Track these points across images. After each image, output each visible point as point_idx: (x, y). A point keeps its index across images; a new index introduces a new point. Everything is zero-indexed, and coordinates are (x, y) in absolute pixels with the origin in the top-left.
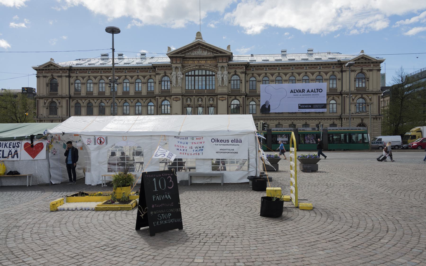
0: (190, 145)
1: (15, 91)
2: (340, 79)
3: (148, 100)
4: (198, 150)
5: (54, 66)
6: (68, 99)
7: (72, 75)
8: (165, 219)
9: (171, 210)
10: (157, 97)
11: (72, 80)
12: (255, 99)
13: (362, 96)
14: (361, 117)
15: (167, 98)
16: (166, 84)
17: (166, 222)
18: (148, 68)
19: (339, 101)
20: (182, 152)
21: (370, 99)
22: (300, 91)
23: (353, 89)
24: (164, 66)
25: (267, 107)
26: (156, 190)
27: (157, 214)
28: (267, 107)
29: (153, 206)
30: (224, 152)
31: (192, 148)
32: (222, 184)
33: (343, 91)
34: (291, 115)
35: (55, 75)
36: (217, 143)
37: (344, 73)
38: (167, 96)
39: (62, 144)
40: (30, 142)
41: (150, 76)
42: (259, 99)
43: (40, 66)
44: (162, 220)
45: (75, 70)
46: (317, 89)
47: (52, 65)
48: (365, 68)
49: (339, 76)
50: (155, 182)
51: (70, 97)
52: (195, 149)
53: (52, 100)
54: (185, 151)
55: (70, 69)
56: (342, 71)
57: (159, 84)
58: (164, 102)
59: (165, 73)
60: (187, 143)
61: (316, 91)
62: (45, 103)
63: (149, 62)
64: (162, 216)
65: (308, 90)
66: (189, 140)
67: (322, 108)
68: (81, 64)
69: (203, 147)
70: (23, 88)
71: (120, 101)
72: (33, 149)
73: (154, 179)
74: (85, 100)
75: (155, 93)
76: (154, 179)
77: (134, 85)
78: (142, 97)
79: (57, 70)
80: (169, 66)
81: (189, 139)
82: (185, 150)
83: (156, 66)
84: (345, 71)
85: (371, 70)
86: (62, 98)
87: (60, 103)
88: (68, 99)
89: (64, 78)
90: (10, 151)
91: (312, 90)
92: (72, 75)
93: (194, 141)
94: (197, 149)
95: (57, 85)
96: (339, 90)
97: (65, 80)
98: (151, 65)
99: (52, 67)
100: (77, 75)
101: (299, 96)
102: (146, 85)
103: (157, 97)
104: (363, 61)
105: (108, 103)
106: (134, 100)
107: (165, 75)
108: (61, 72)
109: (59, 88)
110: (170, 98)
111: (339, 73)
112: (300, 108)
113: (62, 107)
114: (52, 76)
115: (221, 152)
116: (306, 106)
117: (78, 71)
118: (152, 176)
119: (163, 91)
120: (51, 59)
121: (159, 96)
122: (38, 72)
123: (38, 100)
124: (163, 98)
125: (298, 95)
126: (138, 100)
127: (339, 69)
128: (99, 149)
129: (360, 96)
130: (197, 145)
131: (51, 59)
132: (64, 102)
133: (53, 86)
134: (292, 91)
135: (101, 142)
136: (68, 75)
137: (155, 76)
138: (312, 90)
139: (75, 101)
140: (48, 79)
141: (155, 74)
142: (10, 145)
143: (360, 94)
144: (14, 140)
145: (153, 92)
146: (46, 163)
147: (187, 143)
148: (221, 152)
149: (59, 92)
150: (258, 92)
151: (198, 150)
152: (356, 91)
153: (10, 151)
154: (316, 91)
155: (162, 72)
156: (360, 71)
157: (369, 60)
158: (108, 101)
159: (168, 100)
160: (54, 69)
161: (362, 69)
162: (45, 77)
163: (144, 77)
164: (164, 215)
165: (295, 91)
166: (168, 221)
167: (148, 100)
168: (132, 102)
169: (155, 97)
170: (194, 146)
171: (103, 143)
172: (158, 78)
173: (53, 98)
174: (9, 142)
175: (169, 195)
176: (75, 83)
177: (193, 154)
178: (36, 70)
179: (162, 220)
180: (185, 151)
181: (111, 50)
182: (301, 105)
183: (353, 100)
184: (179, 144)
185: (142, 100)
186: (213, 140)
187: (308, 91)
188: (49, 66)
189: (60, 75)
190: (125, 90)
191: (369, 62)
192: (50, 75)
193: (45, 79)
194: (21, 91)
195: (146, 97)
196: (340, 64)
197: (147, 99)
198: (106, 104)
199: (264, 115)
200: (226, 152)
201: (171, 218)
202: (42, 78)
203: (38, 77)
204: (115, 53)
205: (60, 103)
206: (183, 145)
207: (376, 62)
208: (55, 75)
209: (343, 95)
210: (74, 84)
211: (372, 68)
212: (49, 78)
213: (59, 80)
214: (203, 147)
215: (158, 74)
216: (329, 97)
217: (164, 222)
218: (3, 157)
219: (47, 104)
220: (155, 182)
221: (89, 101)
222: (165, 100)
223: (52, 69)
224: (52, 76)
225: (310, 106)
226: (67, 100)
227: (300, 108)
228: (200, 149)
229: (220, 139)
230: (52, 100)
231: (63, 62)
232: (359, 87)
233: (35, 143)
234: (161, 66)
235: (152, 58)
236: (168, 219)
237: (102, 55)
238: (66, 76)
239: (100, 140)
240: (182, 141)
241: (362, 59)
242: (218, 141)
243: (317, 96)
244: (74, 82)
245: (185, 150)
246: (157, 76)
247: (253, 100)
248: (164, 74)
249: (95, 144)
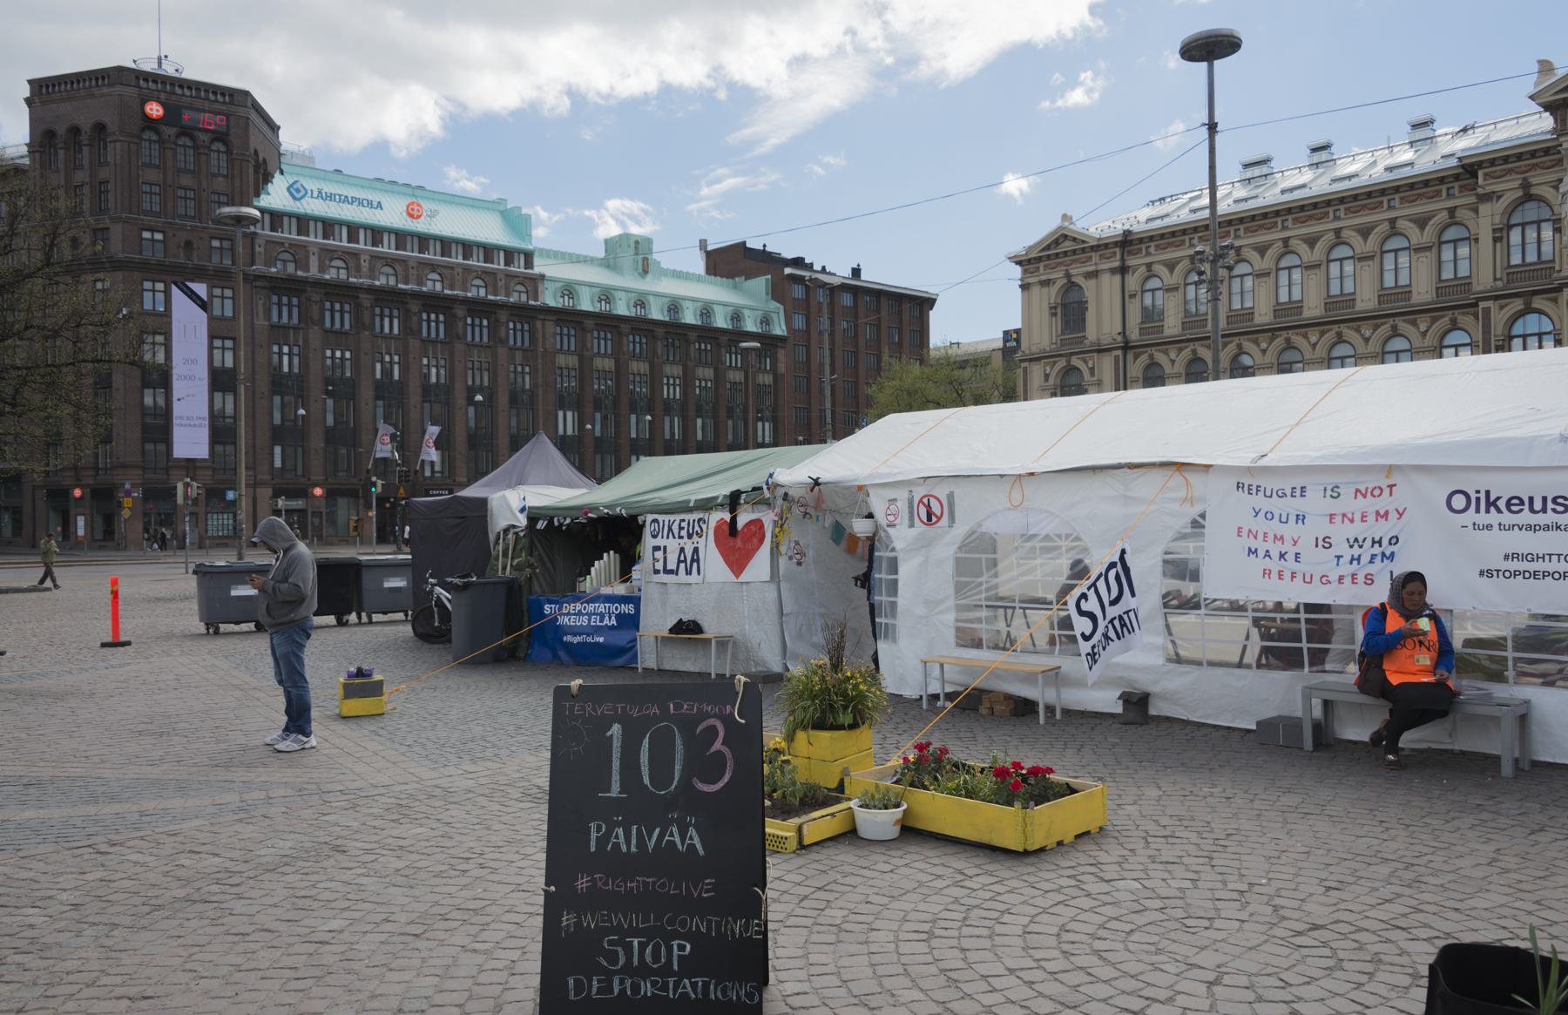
0: (1317, 527)
1: (981, 348)
3: (1444, 322)
4: (1365, 559)
5: (1074, 239)
6: (1119, 352)
7: (1132, 262)
8: (644, 971)
9: (697, 924)
10: (1482, 305)
11: (1133, 282)
15: (1538, 303)
16: (1531, 234)
17: (647, 988)
18: (1442, 180)
20: (1274, 565)
24: (1519, 157)
26: (615, 790)
27: (602, 932)
29: (582, 883)
30: (1535, 575)
31: (1327, 543)
32: (1507, 769)
35: (1077, 271)
36: (1483, 518)
38: (1535, 293)
39: (828, 522)
40: (727, 517)
41: (1452, 211)
43: (1031, 248)
44: (628, 970)
45: (1141, 240)
47: (1066, 237)
50: (616, 745)
51: (1126, 347)
52: (1348, 554)
53: (1068, 362)
54: (1290, 563)
55: (1127, 242)
57: (1495, 240)
58: (1519, 323)
59: (1526, 185)
60: (1301, 518)
62: (1047, 377)
63: (1446, 150)
64: (628, 948)
66: (1315, 503)
68: (1162, 217)
69: (1394, 540)
70: (1006, 333)
71: (1313, 339)
72: (737, 544)
73: (616, 729)
74: (1180, 350)
75: (1476, 288)
76: (616, 729)
77: (1375, 263)
78: (1412, 314)
79: (1083, 250)
80: (1547, 151)
81: (1314, 494)
82: (1290, 557)
83: (1480, 164)
87: (1092, 370)
88: (1119, 352)
90: (682, 550)
92: (1132, 262)
93: (1338, 507)
94: (1356, 551)
95: (1082, 307)
97: (1110, 283)
98: (1453, 162)
99: (1067, 246)
100: (1149, 260)
102: (1432, 255)
103: (1482, 305)
105: (1264, 351)
107: (1528, 197)
108: (1095, 256)
109: (1091, 316)
110: (1555, 301)
114: (1068, 275)
115: (1515, 574)
117: (1152, 244)
118: (605, 709)
119: (1513, 273)
120: (1065, 217)
121: (1497, 298)
122: (1025, 272)
123: (1025, 369)
124: (1518, 305)
126: (1394, 328)
128: (923, 544)
130: (1356, 530)
131: (1065, 217)
133: (1071, 312)
135: (929, 515)
136: (1117, 264)
137: (1476, 211)
139: (1144, 359)
140: (1054, 289)
141: (1473, 199)
142: (681, 528)
144: (690, 510)
145: (1465, 284)
146: (771, 594)
147: (1301, 518)
148: (1515, 574)
149: (1091, 333)
151: (1365, 559)
153: (682, 550)
155: (1509, 187)
158: (1264, 345)
159: (1540, 312)
160: (1074, 252)
162: (1046, 283)
163: (1422, 222)
164: (642, 946)
166: (665, 988)
167: (1444, 322)
168: (1367, 340)
169: (1476, 305)
170: (1341, 533)
171: (939, 519)
172: (1489, 215)
173: (1072, 354)
174: (678, 517)
175: (692, 832)
176: (1143, 292)
177: (1334, 577)
178: (1019, 263)
179: (628, 970)
180: (1290, 563)
181: (1204, 132)
184: (1260, 525)
185: (1414, 323)
186: (1459, 501)
188: (1057, 242)
189: (1092, 268)
190: (1335, 290)
192: (1061, 274)
193: (1045, 290)
194: (1000, 344)
195: (1431, 311)
198: (1259, 359)
200: (1545, 574)
201: (689, 967)
202: (1036, 290)
203: (1025, 287)
204: (1218, 138)
205: (1092, 370)
206: (1281, 529)
208: (1077, 271)
210: (1138, 297)
212: (1059, 283)
213: (1089, 287)
214: (1394, 540)
215: (1486, 198)
217: (636, 988)
218: (666, 571)
219: (1051, 381)
220: (616, 745)
221: (1194, 352)
222: (1529, 310)
224: (1068, 275)
226: (1117, 358)
228: (1377, 550)
229: (1503, 488)
230: (1068, 362)
231: (1100, 224)
233: (743, 519)
234: (1506, 159)
235: (1465, 130)
236: (666, 971)
237: (1246, 166)
238: (1113, 271)
239: (928, 507)
240: (1275, 504)
242: (1491, 504)
244: (1138, 288)
245: (1290, 557)
246: (1485, 209)
248: (1520, 193)
249: (912, 525)
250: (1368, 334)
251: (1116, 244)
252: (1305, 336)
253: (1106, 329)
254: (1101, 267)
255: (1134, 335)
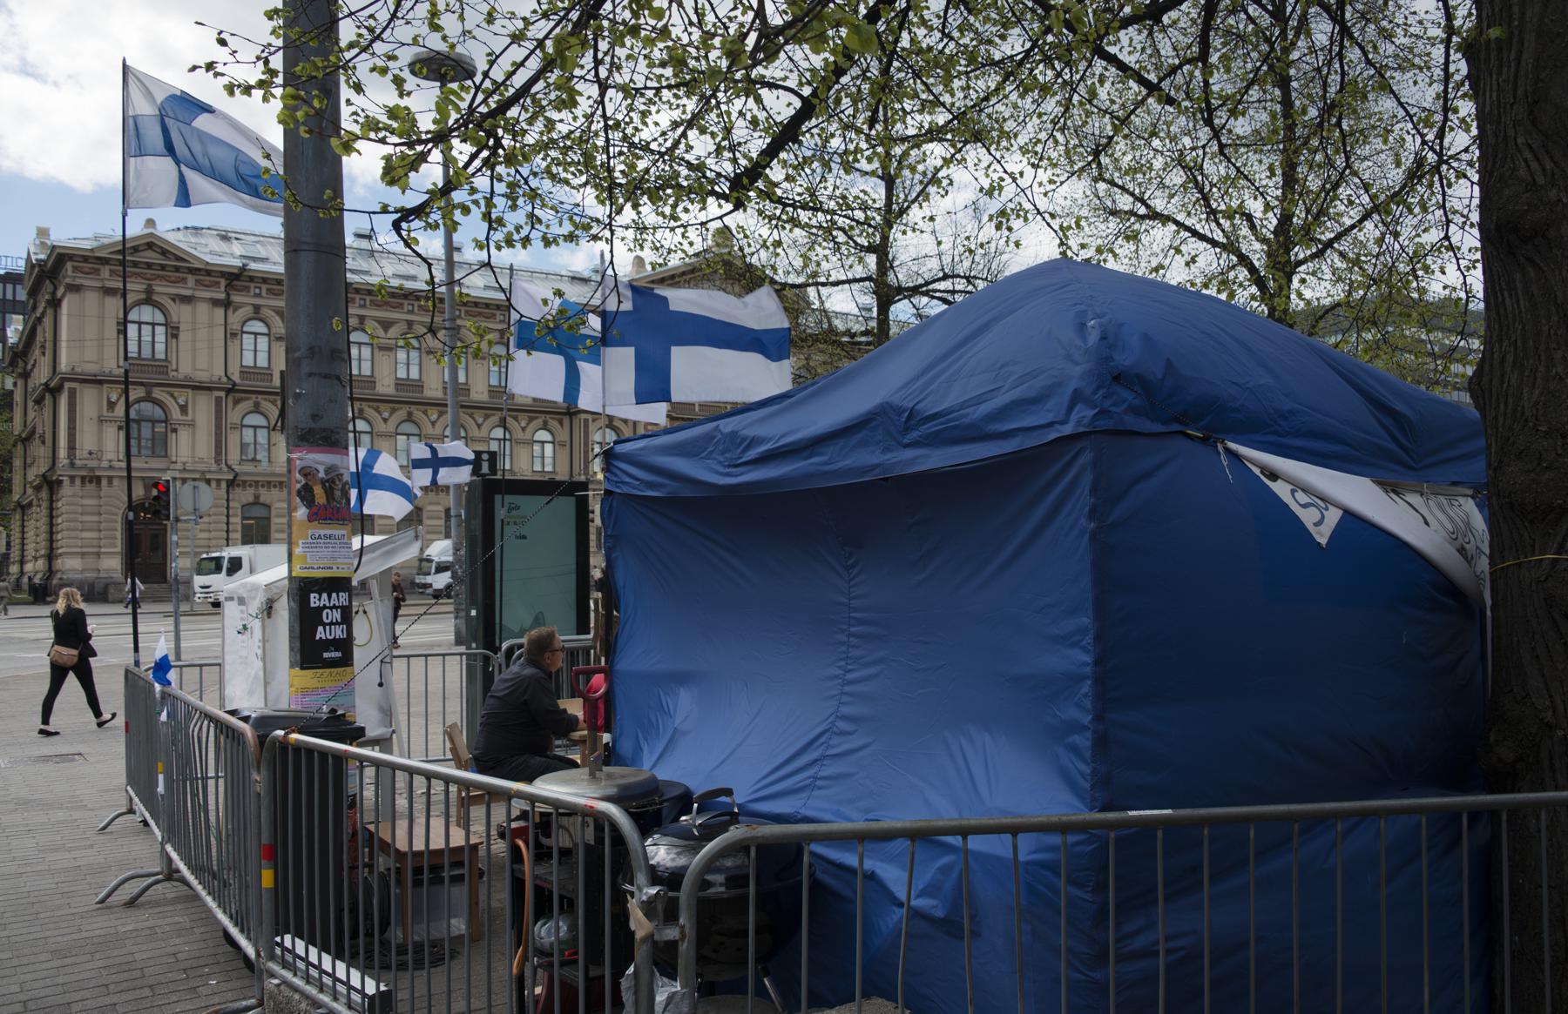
5: (164, 252)
6: (222, 394)
71: (434, 417)
79: (177, 269)
86: (194, 388)
88: (222, 394)
89: (203, 309)
106: (486, 417)
108: (191, 279)
113: (192, 425)
123: (72, 393)
132: (203, 409)
136: (223, 296)
158: (386, 415)
160: (163, 267)
197: (531, 420)
223: (149, 266)
238: (215, 303)
250: (480, 420)
251: (223, 274)
252: (425, 412)
253: (202, 362)
254: (199, 294)
255: (236, 378)
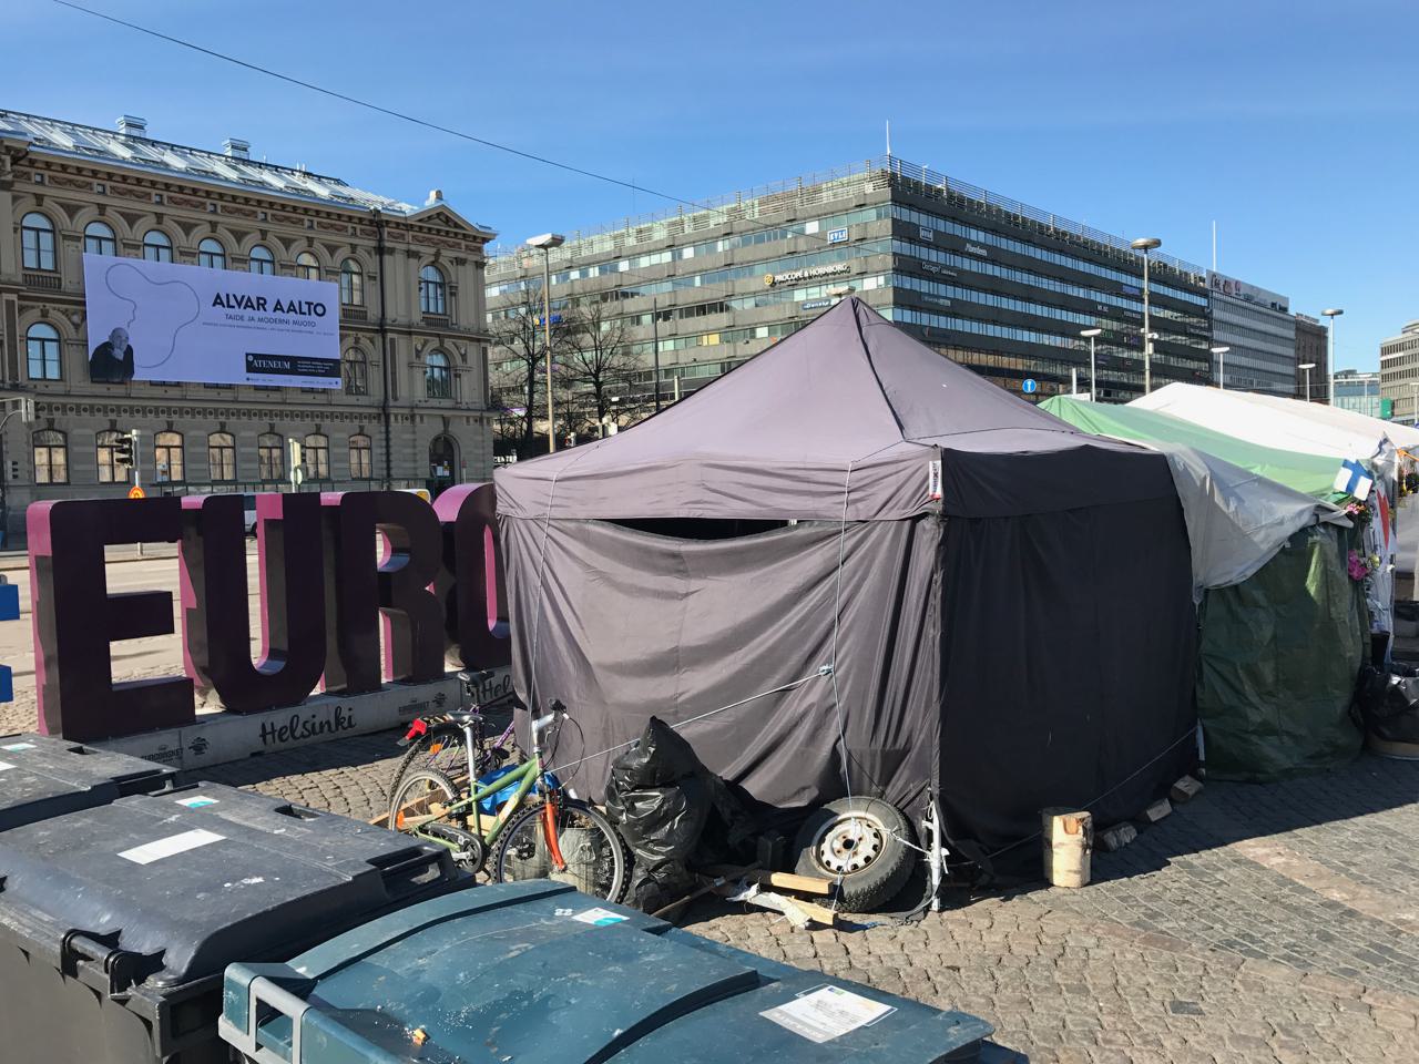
2: (375, 278)
12: (55, 315)
13: (442, 343)
14: (447, 413)
19: (375, 354)
21: (464, 357)
22: (249, 304)
23: (417, 318)
25: (119, 354)
28: (119, 354)
33: (389, 322)
34: (212, 394)
37: (387, 258)
42: (76, 319)
46: (309, 304)
48: (448, 254)
49: (372, 264)
56: (381, 251)
61: (305, 308)
65: (278, 303)
67: (326, 374)
84: (392, 251)
85: (461, 262)
91: (292, 304)
96: (373, 313)
101: (246, 323)
104: (437, 224)
111: (369, 253)
112: (250, 368)
116: (273, 365)
125: (242, 318)
127: (373, 244)
129: (435, 343)
134: (218, 301)
138: (292, 304)
143: (438, 335)
150: (68, 284)
152: (423, 324)
154: (305, 308)
156: (432, 259)
157: (456, 225)
161: (437, 255)
165: (233, 302)
182: (256, 356)
183: (418, 353)
187: (278, 307)
191: (456, 234)
196: (376, 223)
199: (100, 389)
207: (475, 238)
209: (390, 335)
211: (462, 255)
216: (342, 337)
225: (287, 365)
227: (250, 368)
232: (428, 312)
241: (437, 221)
243: (308, 328)
247: (44, 318)
